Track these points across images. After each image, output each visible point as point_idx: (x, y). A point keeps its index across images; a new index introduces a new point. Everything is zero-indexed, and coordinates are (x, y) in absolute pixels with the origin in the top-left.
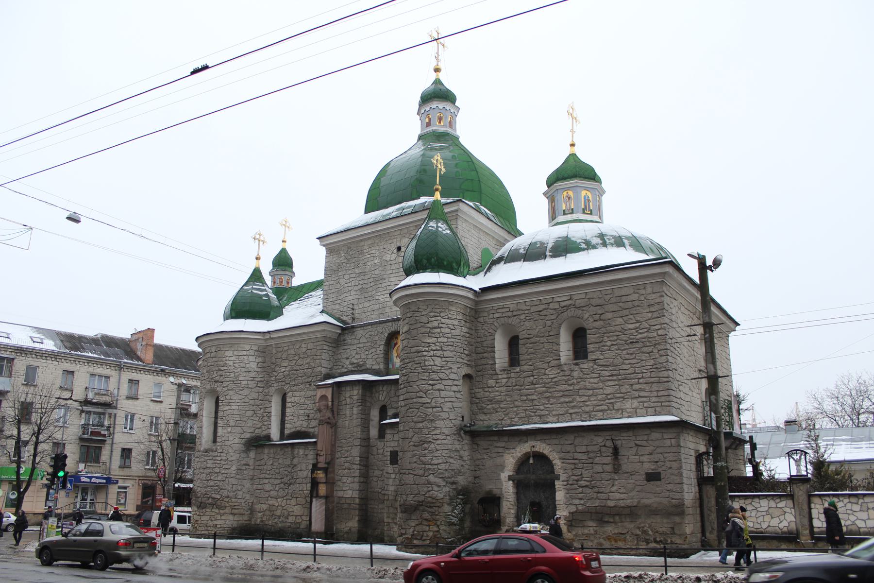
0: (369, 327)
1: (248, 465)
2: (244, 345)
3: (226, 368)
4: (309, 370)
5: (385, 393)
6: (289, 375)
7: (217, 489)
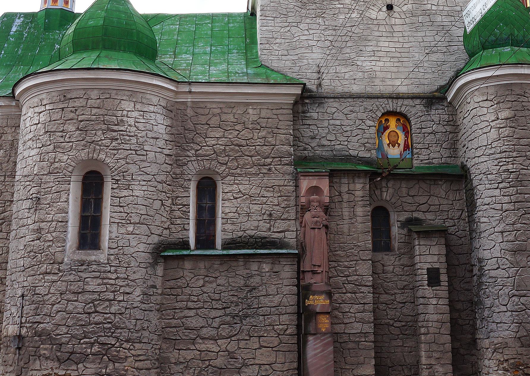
0: (350, 100)
1: (154, 287)
2: (152, 97)
3: (122, 128)
4: (265, 148)
5: (391, 191)
6: (225, 150)
7: (110, 328)
